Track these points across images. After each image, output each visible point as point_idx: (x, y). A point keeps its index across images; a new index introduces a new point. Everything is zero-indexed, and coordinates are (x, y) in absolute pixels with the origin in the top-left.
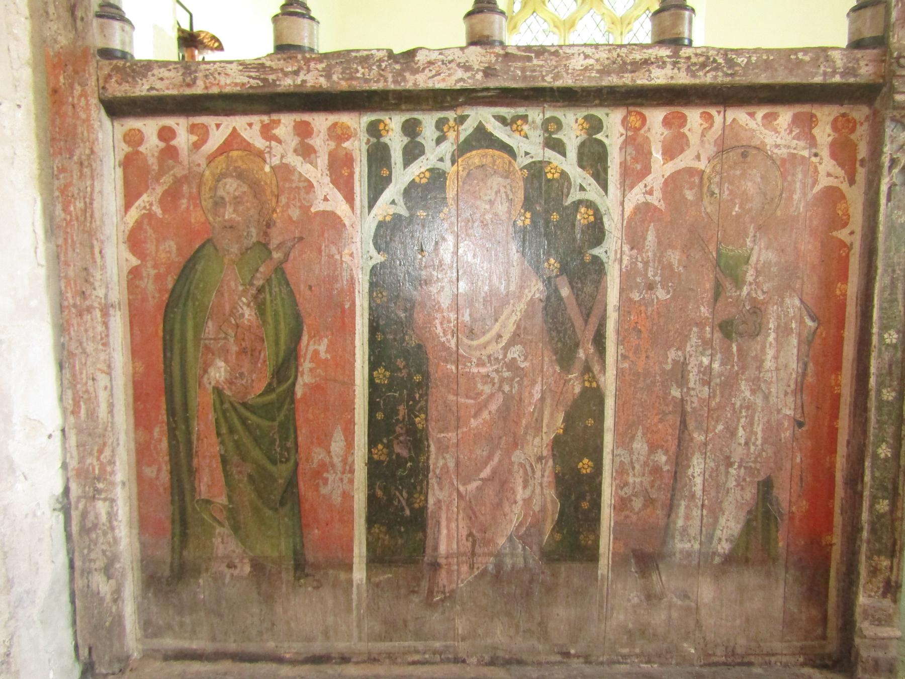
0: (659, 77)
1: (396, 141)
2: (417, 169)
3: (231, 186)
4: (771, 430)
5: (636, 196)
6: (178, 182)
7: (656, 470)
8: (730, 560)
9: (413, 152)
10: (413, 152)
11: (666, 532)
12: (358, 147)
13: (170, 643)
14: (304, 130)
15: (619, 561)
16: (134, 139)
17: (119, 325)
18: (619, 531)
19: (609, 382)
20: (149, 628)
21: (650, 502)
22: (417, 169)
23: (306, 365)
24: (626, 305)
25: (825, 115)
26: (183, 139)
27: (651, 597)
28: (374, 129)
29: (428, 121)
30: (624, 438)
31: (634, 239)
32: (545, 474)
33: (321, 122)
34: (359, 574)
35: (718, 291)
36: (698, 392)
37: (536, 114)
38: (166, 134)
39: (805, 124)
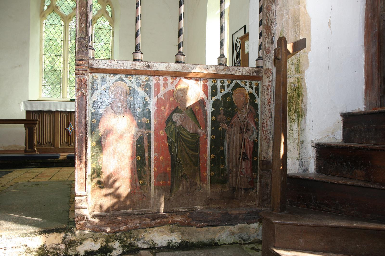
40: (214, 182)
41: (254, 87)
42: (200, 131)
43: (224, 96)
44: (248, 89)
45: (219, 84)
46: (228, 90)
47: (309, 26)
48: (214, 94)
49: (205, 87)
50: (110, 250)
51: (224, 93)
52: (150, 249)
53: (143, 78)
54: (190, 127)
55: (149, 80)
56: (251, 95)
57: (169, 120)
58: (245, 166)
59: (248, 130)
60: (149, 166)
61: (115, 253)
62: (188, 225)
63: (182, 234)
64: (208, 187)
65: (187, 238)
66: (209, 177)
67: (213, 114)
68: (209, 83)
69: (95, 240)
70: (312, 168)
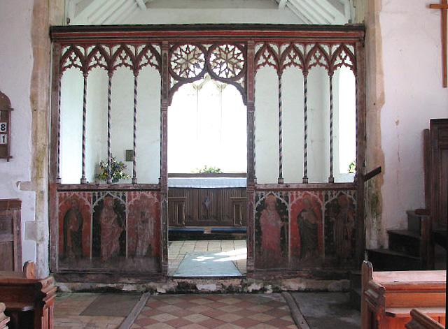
0: (131, 188)
1: (97, 196)
2: (100, 199)
3: (74, 201)
4: (150, 237)
5: (130, 203)
6: (67, 201)
7: (134, 243)
8: (145, 256)
9: (99, 197)
10: (99, 197)
11: (135, 252)
12: (92, 196)
13: (63, 268)
14: (84, 194)
15: (129, 256)
16: (61, 194)
17: (57, 220)
18: (129, 252)
19: (127, 229)
20: (59, 266)
21: (133, 247)
22: (100, 199)
23: (83, 226)
24: (128, 218)
25: (155, 193)
26: (67, 195)
27: (134, 262)
28: (94, 194)
29: (101, 193)
30: (129, 238)
31: (130, 209)
32: (118, 243)
33: (86, 193)
34: (91, 258)
35: (141, 216)
36: (139, 231)
37: (116, 192)
38: (65, 194)
39: (153, 194)
40: (326, 254)
41: (352, 194)
42: (318, 222)
43: (333, 201)
44: (348, 195)
45: (329, 194)
46: (335, 197)
47: (384, 158)
48: (326, 200)
49: (321, 196)
50: (266, 290)
51: (333, 199)
52: (288, 291)
53: (284, 193)
54: (312, 220)
55: (287, 194)
56: (351, 199)
57: (299, 216)
58: (347, 244)
59: (348, 221)
60: (288, 243)
61: (268, 292)
62: (311, 278)
63: (307, 283)
64: (323, 256)
65: (310, 286)
66: (324, 250)
67: (326, 211)
68: (323, 193)
69: (258, 284)
70: (386, 245)
